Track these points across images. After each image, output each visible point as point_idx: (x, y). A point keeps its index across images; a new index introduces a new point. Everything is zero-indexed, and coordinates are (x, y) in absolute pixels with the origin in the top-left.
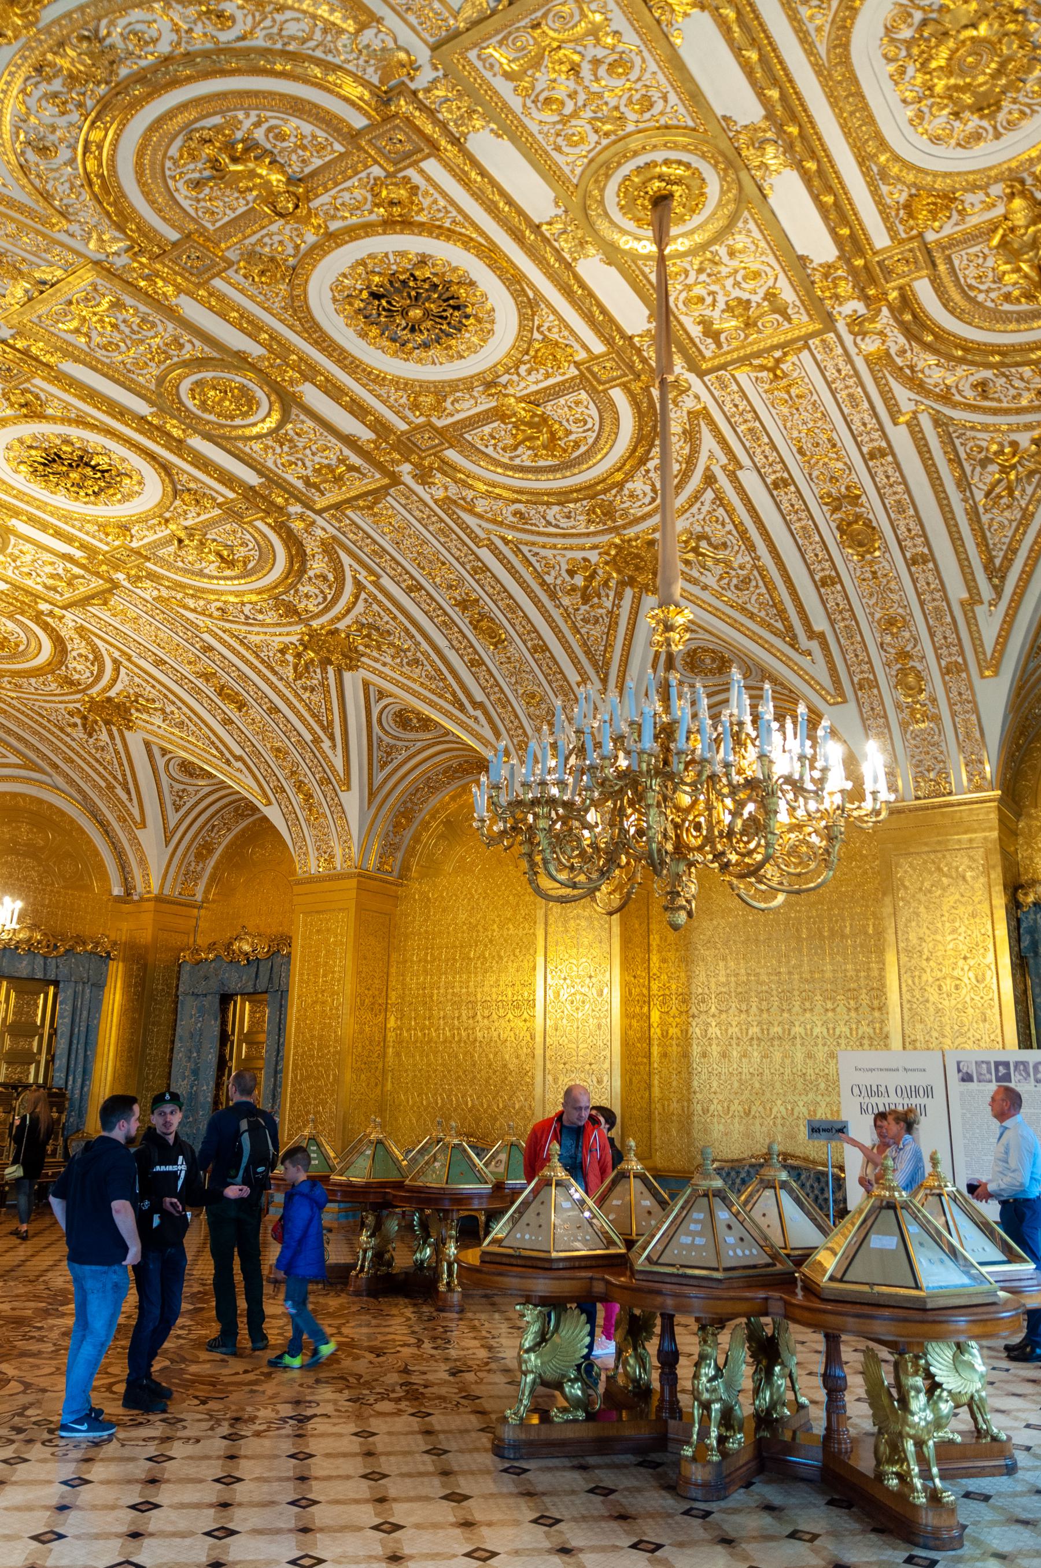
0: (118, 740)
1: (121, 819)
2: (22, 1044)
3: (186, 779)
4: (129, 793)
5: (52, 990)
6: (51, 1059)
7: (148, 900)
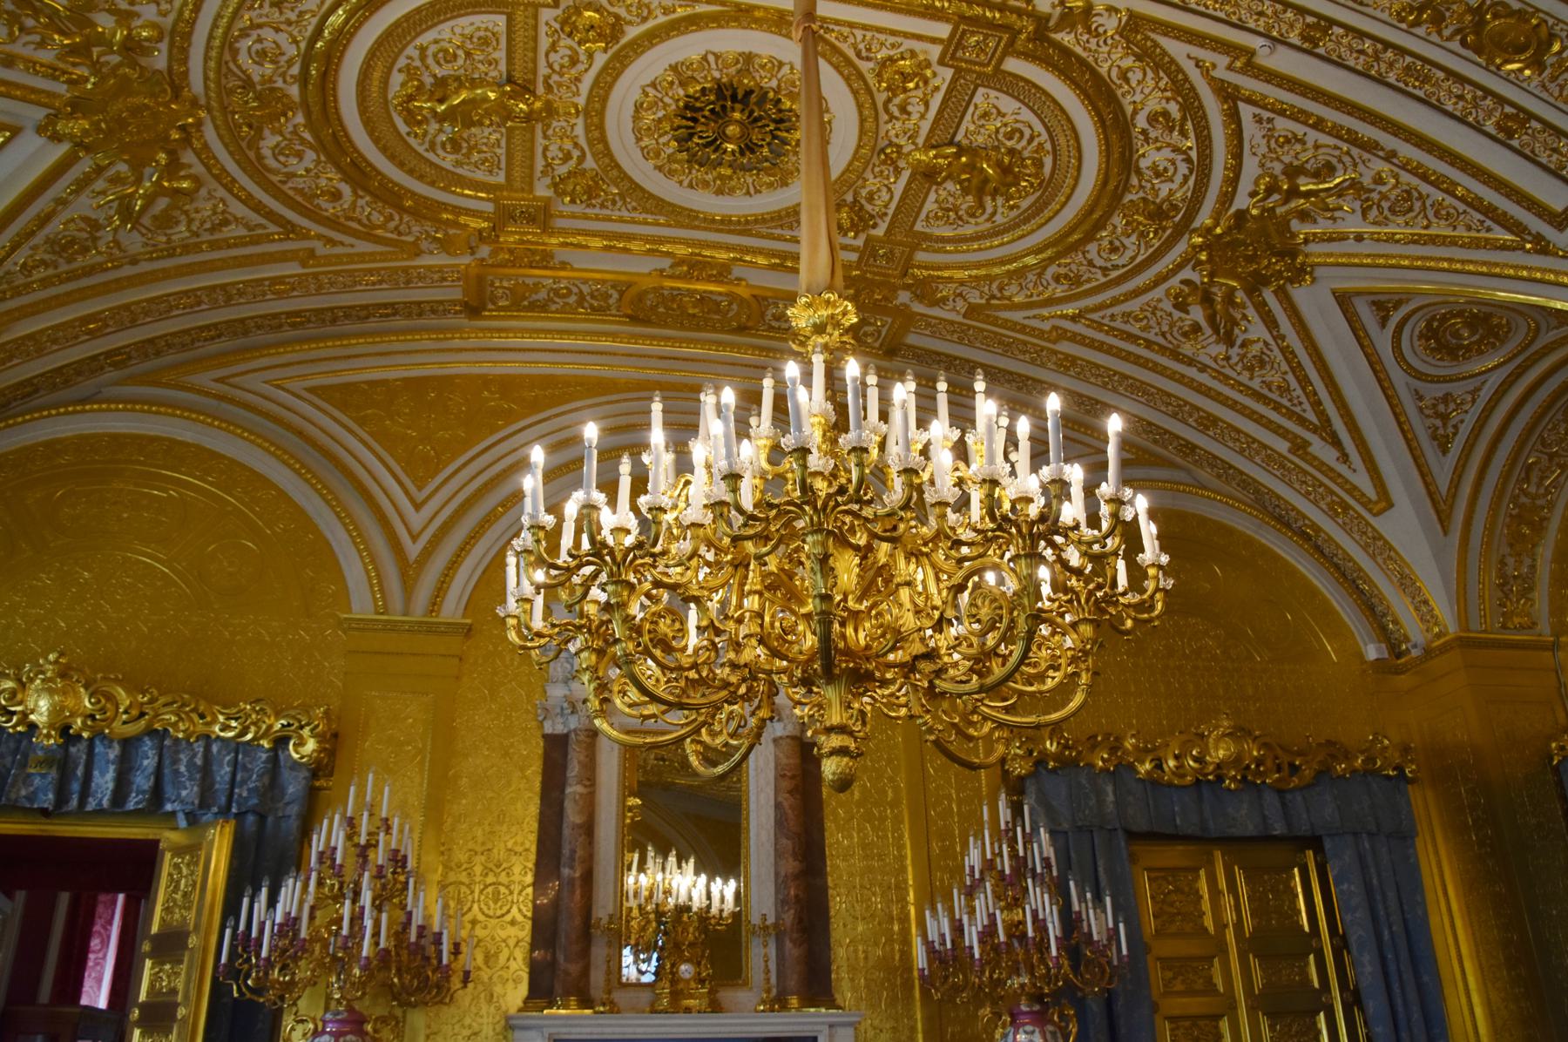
0: (1285, 326)
1: (1337, 509)
3: (1446, 368)
4: (1336, 442)
5: (1310, 853)
7: (1444, 649)
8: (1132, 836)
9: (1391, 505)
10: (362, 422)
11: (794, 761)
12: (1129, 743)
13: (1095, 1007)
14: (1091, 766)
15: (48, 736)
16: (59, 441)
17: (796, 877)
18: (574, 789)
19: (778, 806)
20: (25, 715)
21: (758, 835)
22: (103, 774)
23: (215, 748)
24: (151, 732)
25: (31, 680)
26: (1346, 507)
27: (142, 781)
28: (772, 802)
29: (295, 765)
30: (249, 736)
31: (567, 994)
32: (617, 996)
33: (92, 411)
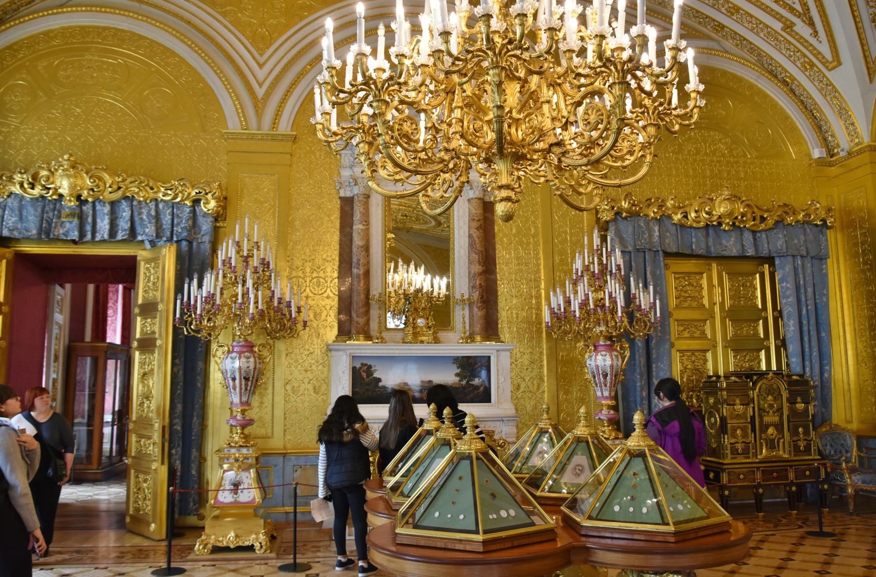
1: (808, 67)
2: (746, 330)
4: (811, 24)
5: (766, 266)
6: (782, 344)
7: (860, 152)
8: (667, 254)
9: (840, 64)
10: (224, 14)
11: (480, 211)
12: (670, 203)
13: (640, 344)
14: (647, 215)
15: (70, 201)
16: (52, 31)
17: (480, 274)
18: (358, 227)
19: (470, 236)
20: (56, 190)
21: (459, 251)
22: (102, 221)
23: (161, 206)
24: (126, 198)
25: (56, 170)
26: (813, 65)
27: (124, 224)
28: (467, 234)
29: (205, 215)
30: (179, 199)
31: (358, 333)
32: (384, 334)
33: (68, 12)
